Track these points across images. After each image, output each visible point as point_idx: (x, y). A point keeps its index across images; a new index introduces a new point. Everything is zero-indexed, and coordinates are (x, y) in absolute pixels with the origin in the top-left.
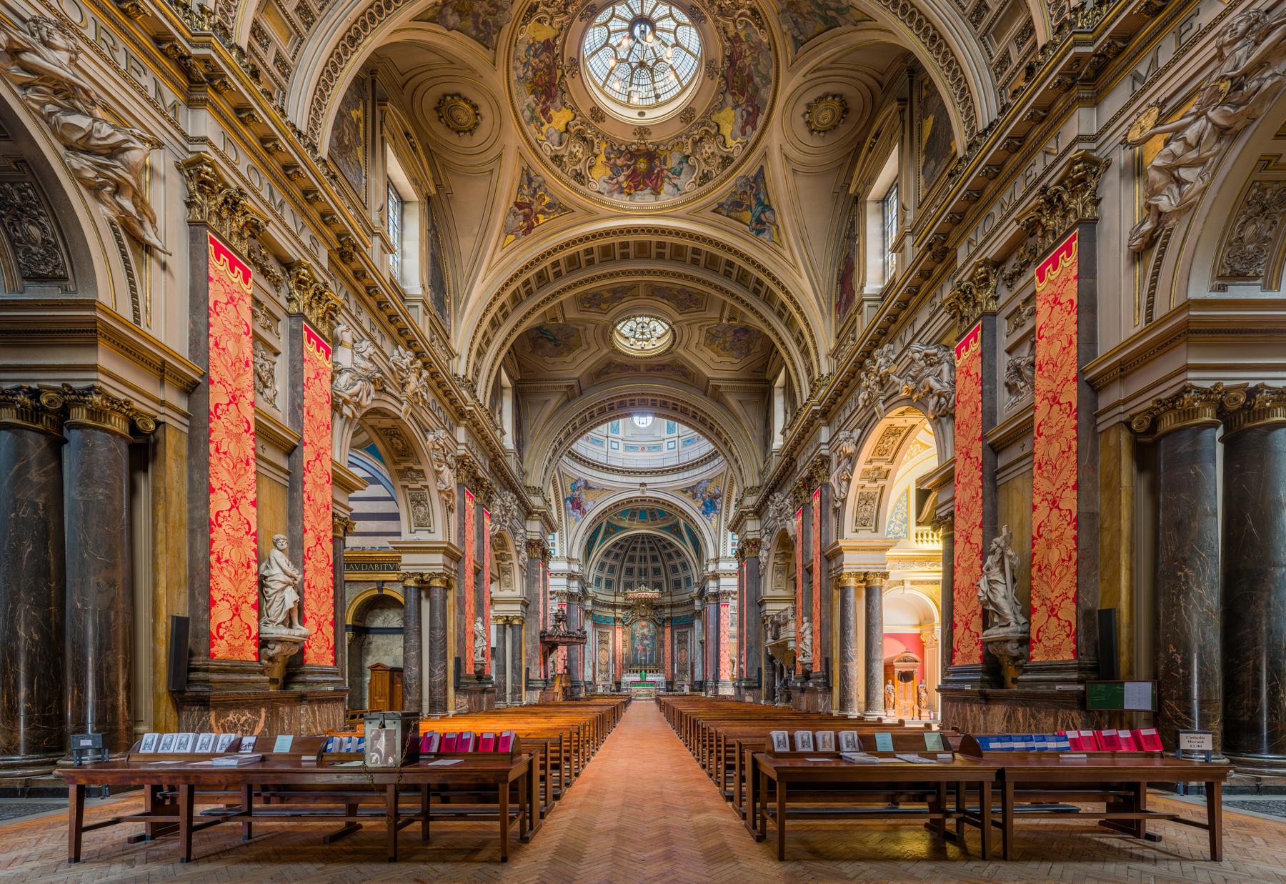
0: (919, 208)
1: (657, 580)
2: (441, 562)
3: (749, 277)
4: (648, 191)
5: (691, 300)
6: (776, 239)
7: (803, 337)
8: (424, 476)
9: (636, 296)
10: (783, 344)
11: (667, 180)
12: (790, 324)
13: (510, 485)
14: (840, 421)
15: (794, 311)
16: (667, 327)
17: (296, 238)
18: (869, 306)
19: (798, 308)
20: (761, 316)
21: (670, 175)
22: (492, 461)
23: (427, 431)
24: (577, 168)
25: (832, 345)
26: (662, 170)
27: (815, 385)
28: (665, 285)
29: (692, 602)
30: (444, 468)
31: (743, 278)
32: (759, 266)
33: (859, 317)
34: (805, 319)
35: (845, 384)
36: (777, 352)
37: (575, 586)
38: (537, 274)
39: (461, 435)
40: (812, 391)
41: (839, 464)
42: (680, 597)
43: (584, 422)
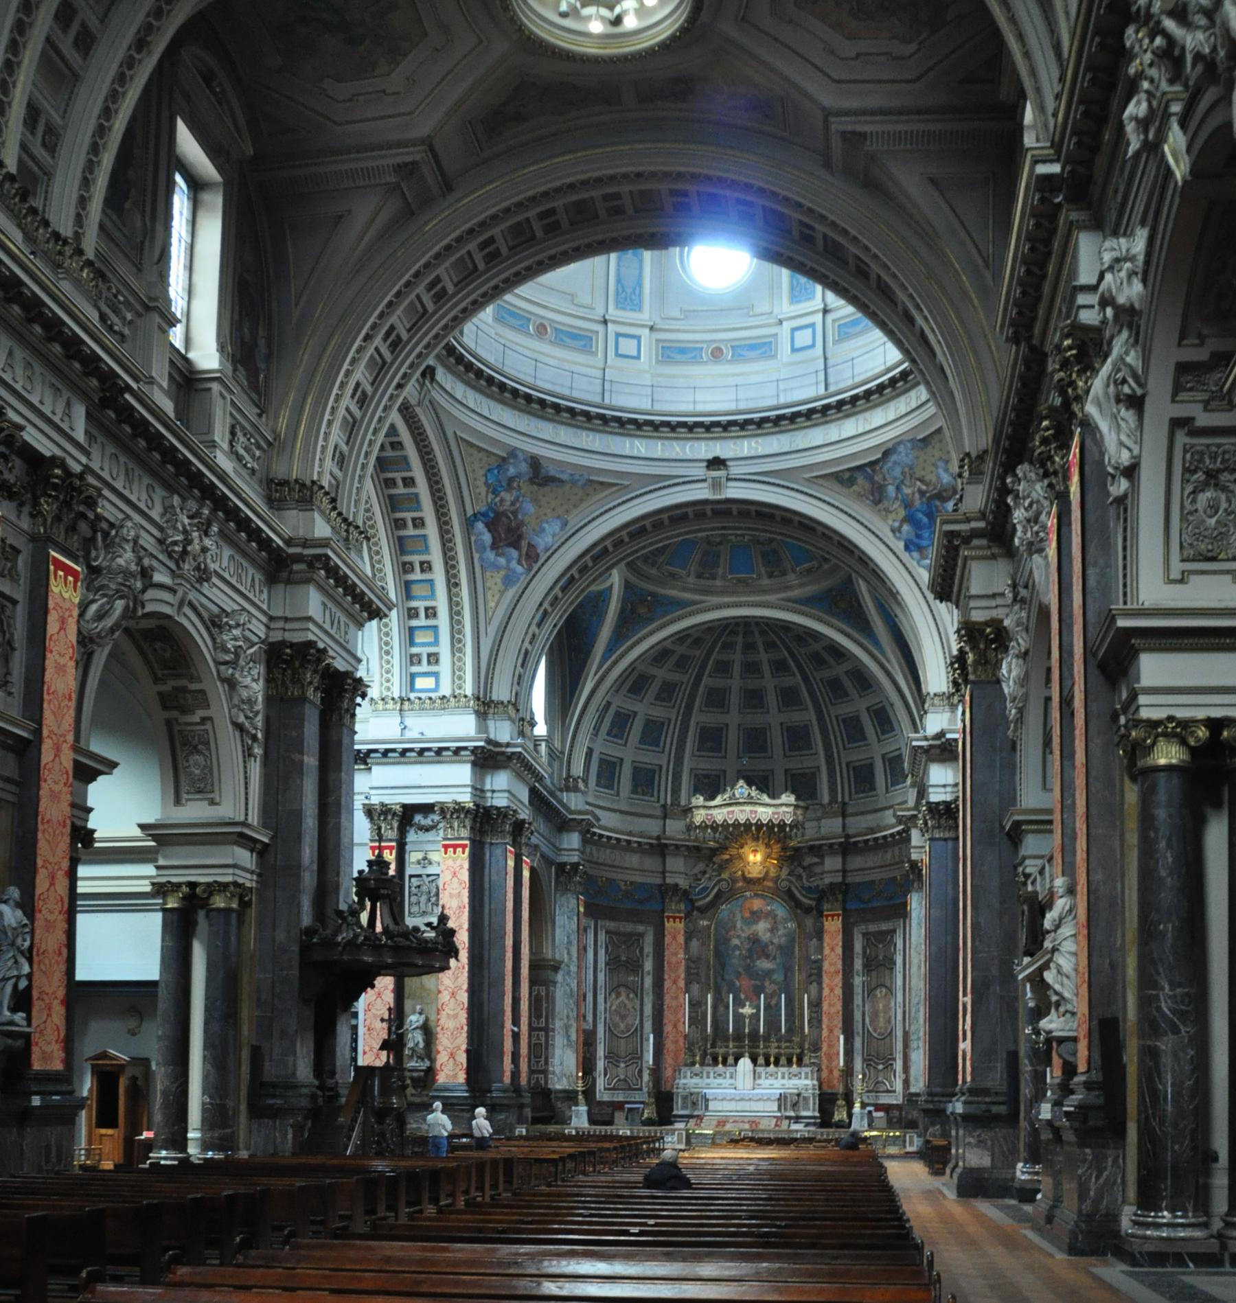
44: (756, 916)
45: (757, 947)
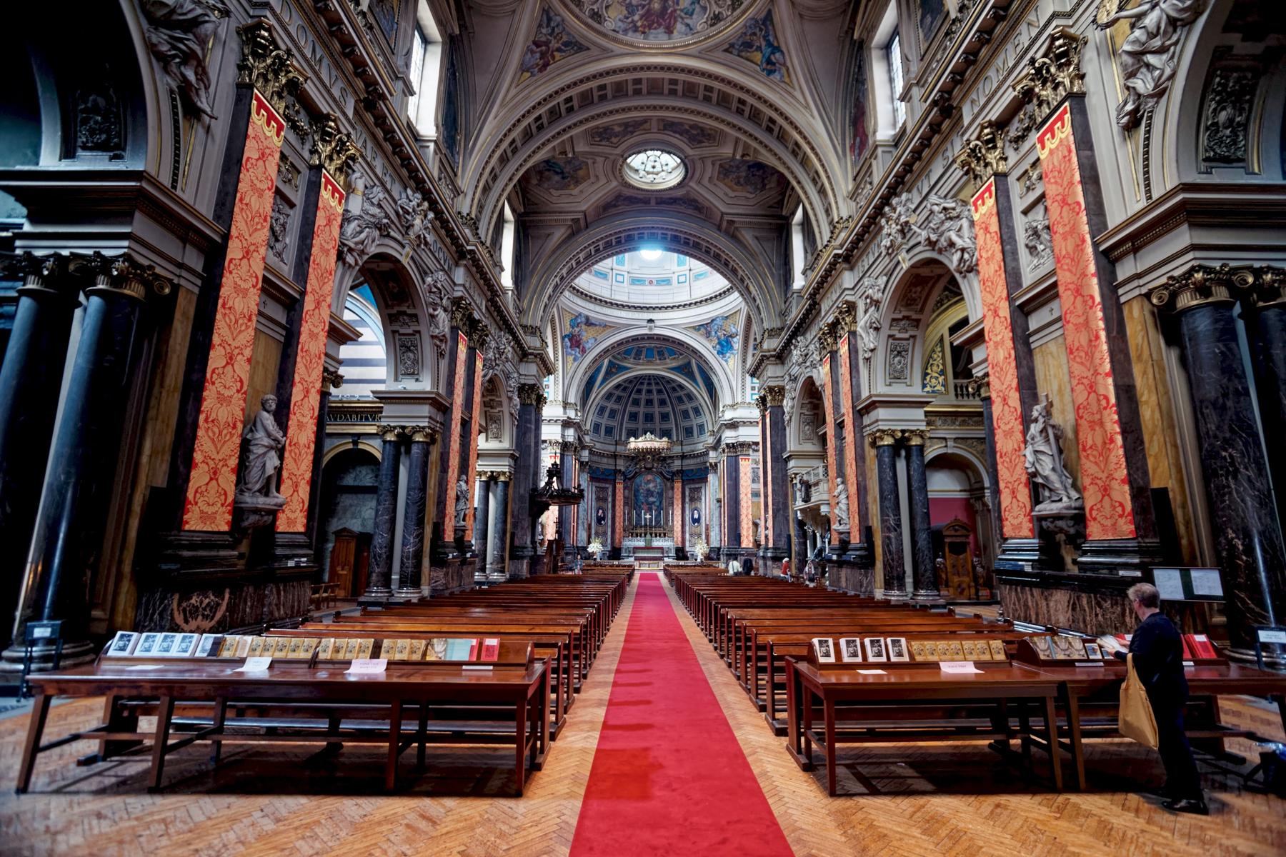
0: (922, 60)
1: (665, 426)
2: (427, 414)
3: (762, 116)
4: (661, 30)
5: (704, 135)
6: (787, 80)
7: (819, 177)
8: (417, 321)
9: (648, 131)
10: (799, 182)
11: (680, 20)
12: (804, 162)
13: (506, 326)
14: (863, 266)
15: (809, 151)
16: (679, 161)
17: (328, 91)
18: (883, 152)
19: (813, 149)
20: (775, 154)
21: (682, 14)
22: (488, 301)
23: (426, 273)
24: (595, 7)
25: (850, 187)
26: (675, 11)
27: (835, 227)
28: (676, 120)
29: (706, 454)
30: (440, 312)
31: (755, 116)
32: (771, 106)
33: (874, 163)
34: (820, 160)
35: (866, 228)
36: (793, 188)
37: (571, 435)
38: (549, 109)
39: (460, 275)
40: (832, 232)
41: (866, 312)
42: (692, 447)
43: (589, 256)
44: (649, 482)
45: (650, 493)
